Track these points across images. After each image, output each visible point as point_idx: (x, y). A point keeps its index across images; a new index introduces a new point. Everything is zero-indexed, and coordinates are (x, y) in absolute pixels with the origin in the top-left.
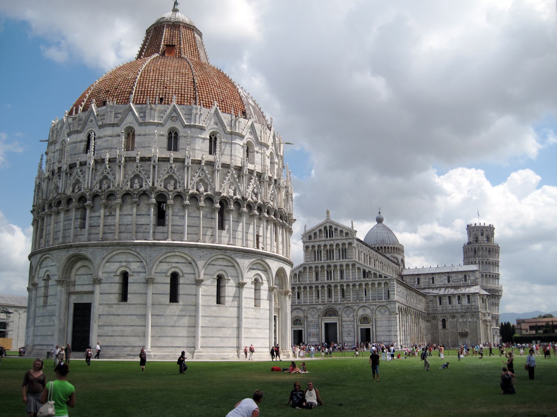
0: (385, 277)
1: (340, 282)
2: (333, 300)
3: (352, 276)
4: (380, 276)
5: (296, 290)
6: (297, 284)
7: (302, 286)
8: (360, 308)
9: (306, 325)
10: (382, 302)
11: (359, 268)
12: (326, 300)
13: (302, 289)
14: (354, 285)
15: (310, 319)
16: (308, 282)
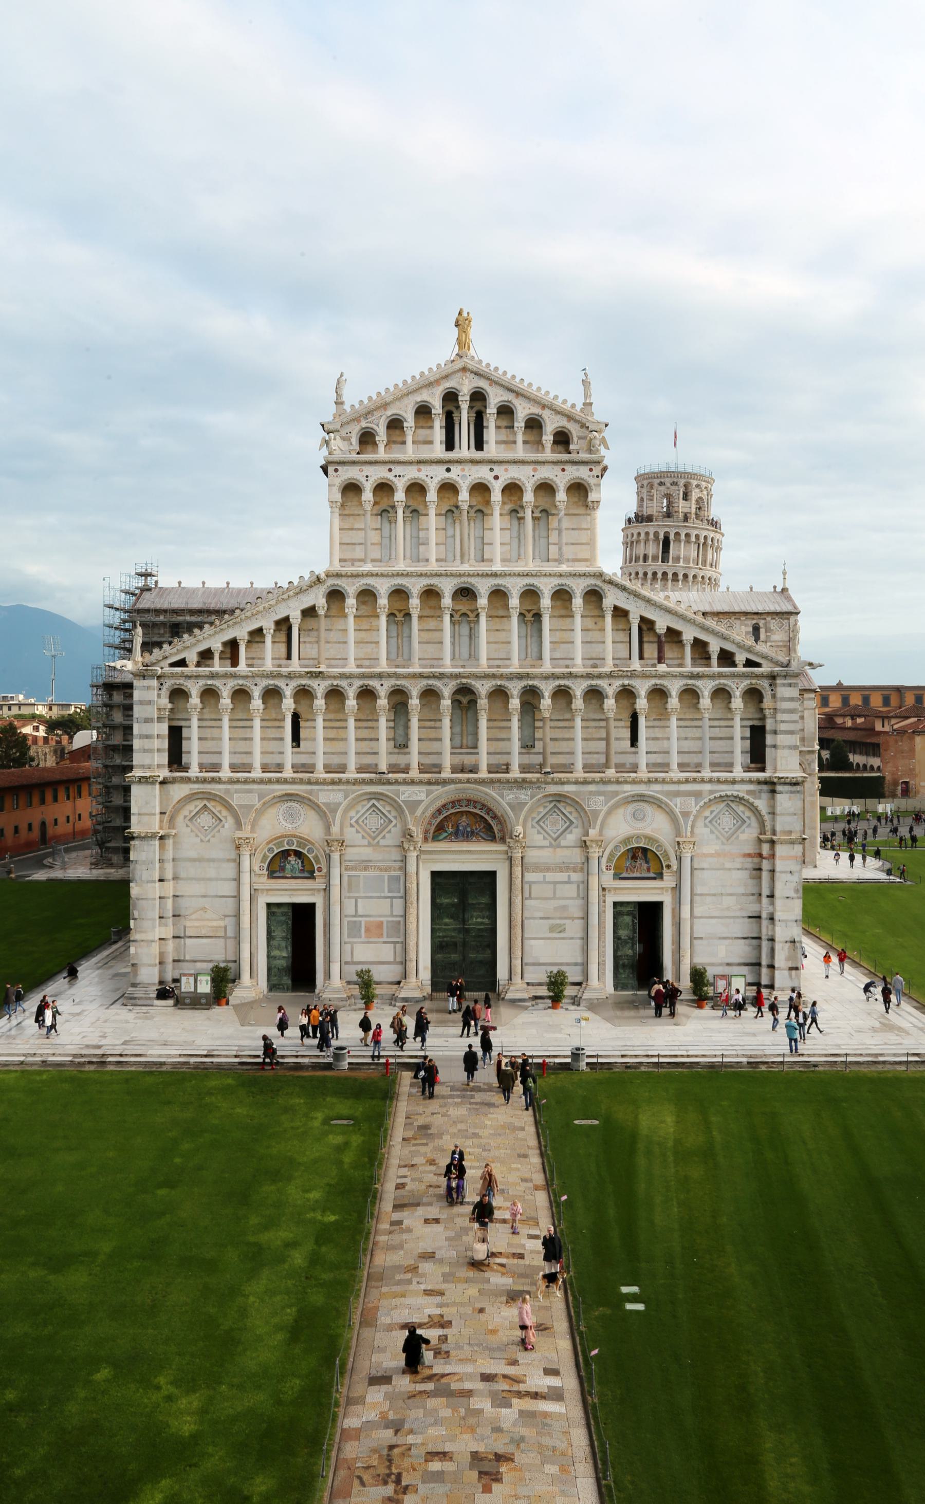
0: (749, 663)
1: (520, 677)
2: (484, 761)
3: (580, 648)
4: (726, 658)
5: (288, 704)
6: (290, 676)
7: (320, 688)
8: (616, 806)
9: (335, 881)
10: (734, 782)
11: (620, 613)
12: (447, 761)
13: (320, 703)
14: (595, 695)
15: (359, 851)
16: (351, 668)
